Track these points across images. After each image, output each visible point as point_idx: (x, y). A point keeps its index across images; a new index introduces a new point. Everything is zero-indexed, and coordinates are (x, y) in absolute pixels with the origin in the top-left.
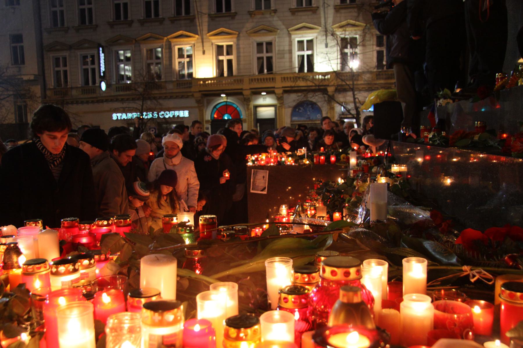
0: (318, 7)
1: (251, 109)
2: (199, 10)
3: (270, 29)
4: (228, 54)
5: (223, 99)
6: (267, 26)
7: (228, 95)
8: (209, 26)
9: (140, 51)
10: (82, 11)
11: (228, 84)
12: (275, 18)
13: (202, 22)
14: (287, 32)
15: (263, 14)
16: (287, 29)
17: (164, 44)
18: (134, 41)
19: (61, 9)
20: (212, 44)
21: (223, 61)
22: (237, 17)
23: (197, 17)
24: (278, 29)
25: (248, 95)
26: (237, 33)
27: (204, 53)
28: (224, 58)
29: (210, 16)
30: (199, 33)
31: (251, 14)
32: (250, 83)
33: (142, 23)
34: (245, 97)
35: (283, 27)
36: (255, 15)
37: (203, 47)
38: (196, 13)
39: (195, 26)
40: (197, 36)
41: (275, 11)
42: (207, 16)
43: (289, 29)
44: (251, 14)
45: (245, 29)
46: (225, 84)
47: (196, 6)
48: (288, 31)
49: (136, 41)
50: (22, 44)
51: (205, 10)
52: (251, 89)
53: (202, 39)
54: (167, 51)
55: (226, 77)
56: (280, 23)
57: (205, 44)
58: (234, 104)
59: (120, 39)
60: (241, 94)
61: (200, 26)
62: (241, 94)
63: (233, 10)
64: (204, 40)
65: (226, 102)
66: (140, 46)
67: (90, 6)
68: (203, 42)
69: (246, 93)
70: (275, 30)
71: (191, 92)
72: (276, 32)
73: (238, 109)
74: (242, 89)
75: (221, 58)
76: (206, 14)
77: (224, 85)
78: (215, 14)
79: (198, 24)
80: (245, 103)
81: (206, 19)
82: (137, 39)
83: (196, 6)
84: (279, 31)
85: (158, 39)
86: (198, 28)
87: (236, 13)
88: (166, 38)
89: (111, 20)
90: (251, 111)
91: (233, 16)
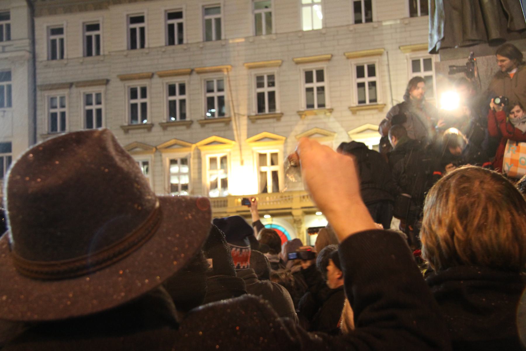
0: (385, 105)
1: (303, 233)
2: (236, 111)
3: (326, 132)
4: (273, 163)
5: (267, 221)
6: (322, 129)
7: (273, 215)
8: (249, 129)
9: (162, 161)
10: (89, 113)
11: (273, 202)
12: (332, 119)
13: (239, 126)
14: (347, 136)
15: (316, 114)
16: (347, 131)
17: (192, 153)
18: (154, 149)
19: (63, 110)
20: (253, 152)
21: (266, 173)
22: (283, 119)
23: (233, 119)
24: (335, 132)
25: (298, 216)
26: (284, 138)
27: (242, 162)
28: (269, 169)
29: (249, 117)
30: (236, 138)
31: (300, 114)
32: (301, 201)
33: (165, 126)
34: (295, 218)
35: (342, 129)
36: (305, 115)
37: (241, 155)
38: (232, 114)
39: (231, 129)
40: (233, 143)
41: (331, 110)
42: (246, 118)
43: (350, 133)
44: (300, 114)
45: (293, 134)
46: (270, 202)
47: (233, 106)
48: (349, 135)
49: (156, 149)
50: (8, 154)
51: (243, 110)
52: (302, 208)
53: (240, 146)
54: (196, 161)
55: (270, 194)
56: (337, 125)
57: (243, 151)
58: (279, 226)
59: (136, 147)
60: (290, 214)
61: (237, 130)
62: (290, 214)
63: (278, 110)
64: (243, 148)
65: (271, 225)
66: (161, 155)
67: (99, 107)
68: (241, 150)
69: (297, 213)
70: (332, 134)
71: (226, 212)
72: (333, 136)
73: (286, 233)
74: (291, 208)
75: (263, 169)
76: (244, 115)
77: (268, 204)
78: (256, 115)
79: (234, 127)
80: (295, 225)
81: (244, 122)
82: (158, 147)
83: (233, 106)
84: (336, 135)
85: (184, 146)
86: (235, 133)
87: (282, 114)
88: (194, 146)
89: (126, 124)
90: (303, 236)
91: (279, 117)
